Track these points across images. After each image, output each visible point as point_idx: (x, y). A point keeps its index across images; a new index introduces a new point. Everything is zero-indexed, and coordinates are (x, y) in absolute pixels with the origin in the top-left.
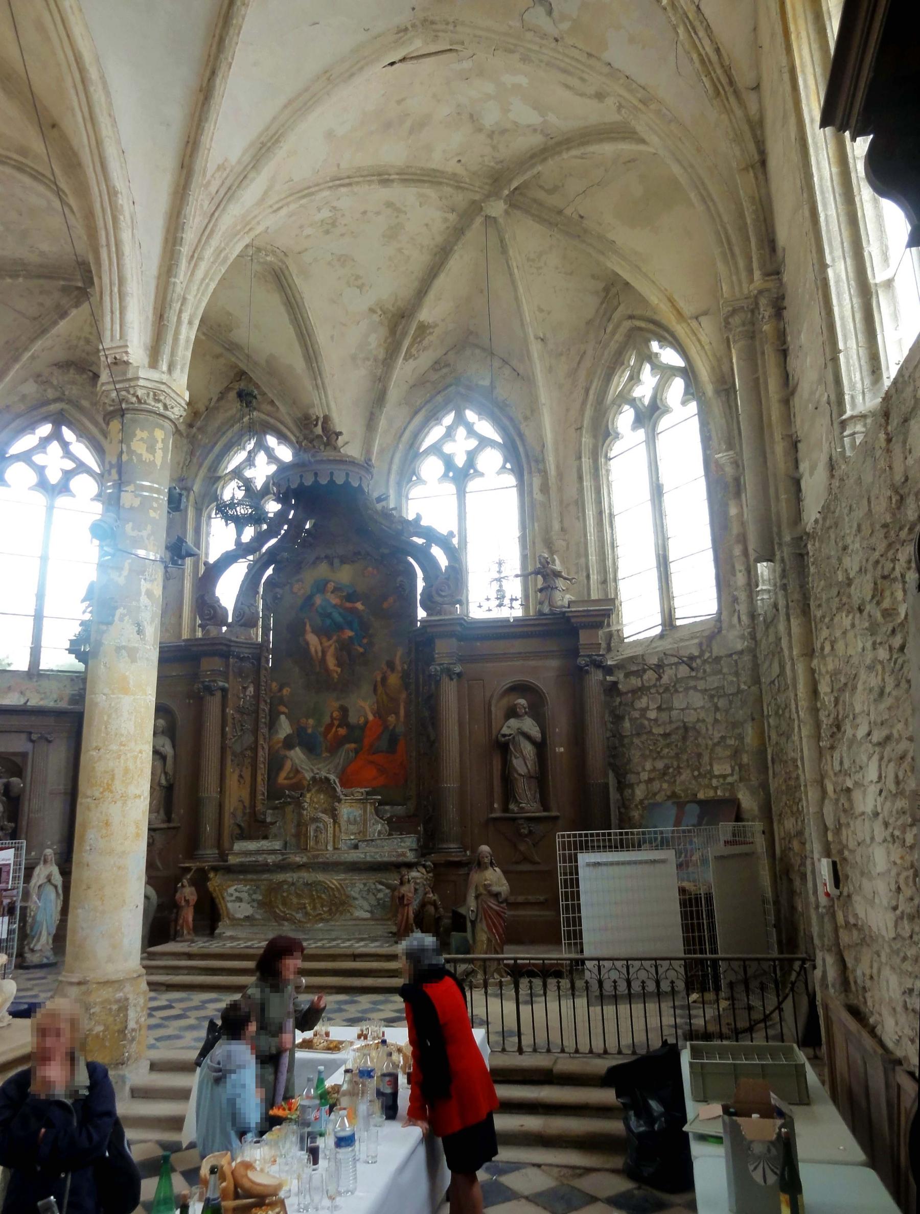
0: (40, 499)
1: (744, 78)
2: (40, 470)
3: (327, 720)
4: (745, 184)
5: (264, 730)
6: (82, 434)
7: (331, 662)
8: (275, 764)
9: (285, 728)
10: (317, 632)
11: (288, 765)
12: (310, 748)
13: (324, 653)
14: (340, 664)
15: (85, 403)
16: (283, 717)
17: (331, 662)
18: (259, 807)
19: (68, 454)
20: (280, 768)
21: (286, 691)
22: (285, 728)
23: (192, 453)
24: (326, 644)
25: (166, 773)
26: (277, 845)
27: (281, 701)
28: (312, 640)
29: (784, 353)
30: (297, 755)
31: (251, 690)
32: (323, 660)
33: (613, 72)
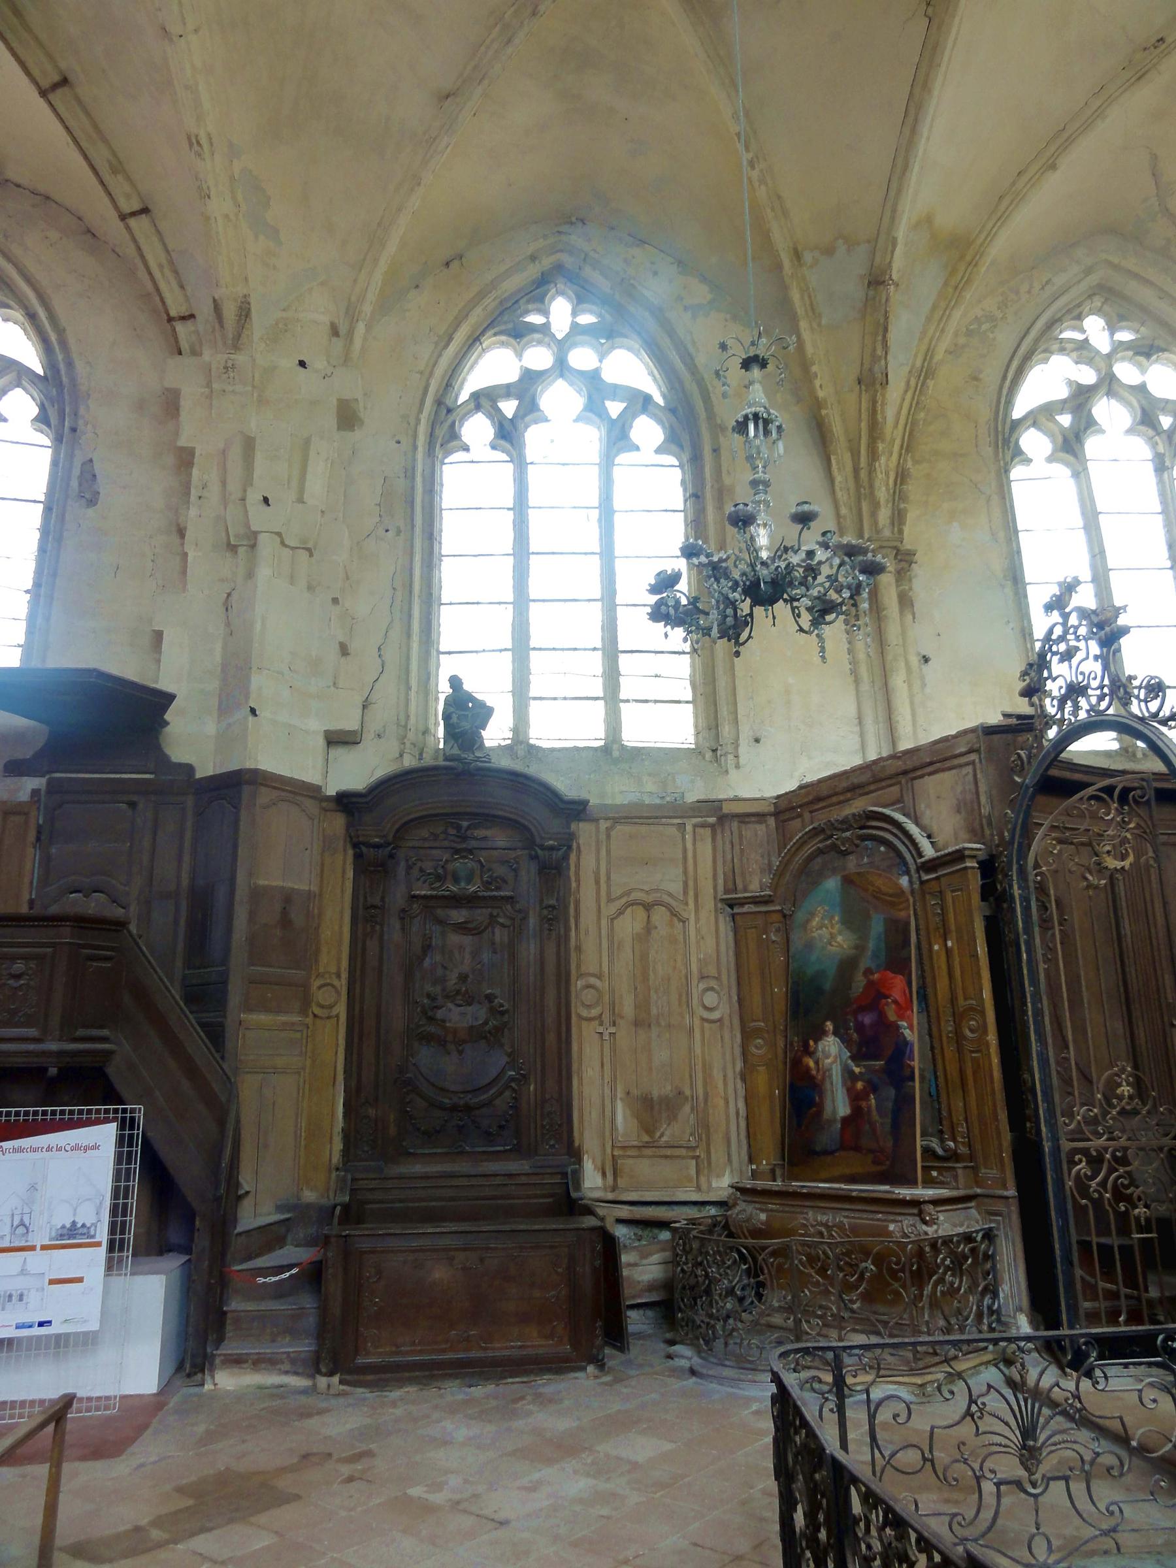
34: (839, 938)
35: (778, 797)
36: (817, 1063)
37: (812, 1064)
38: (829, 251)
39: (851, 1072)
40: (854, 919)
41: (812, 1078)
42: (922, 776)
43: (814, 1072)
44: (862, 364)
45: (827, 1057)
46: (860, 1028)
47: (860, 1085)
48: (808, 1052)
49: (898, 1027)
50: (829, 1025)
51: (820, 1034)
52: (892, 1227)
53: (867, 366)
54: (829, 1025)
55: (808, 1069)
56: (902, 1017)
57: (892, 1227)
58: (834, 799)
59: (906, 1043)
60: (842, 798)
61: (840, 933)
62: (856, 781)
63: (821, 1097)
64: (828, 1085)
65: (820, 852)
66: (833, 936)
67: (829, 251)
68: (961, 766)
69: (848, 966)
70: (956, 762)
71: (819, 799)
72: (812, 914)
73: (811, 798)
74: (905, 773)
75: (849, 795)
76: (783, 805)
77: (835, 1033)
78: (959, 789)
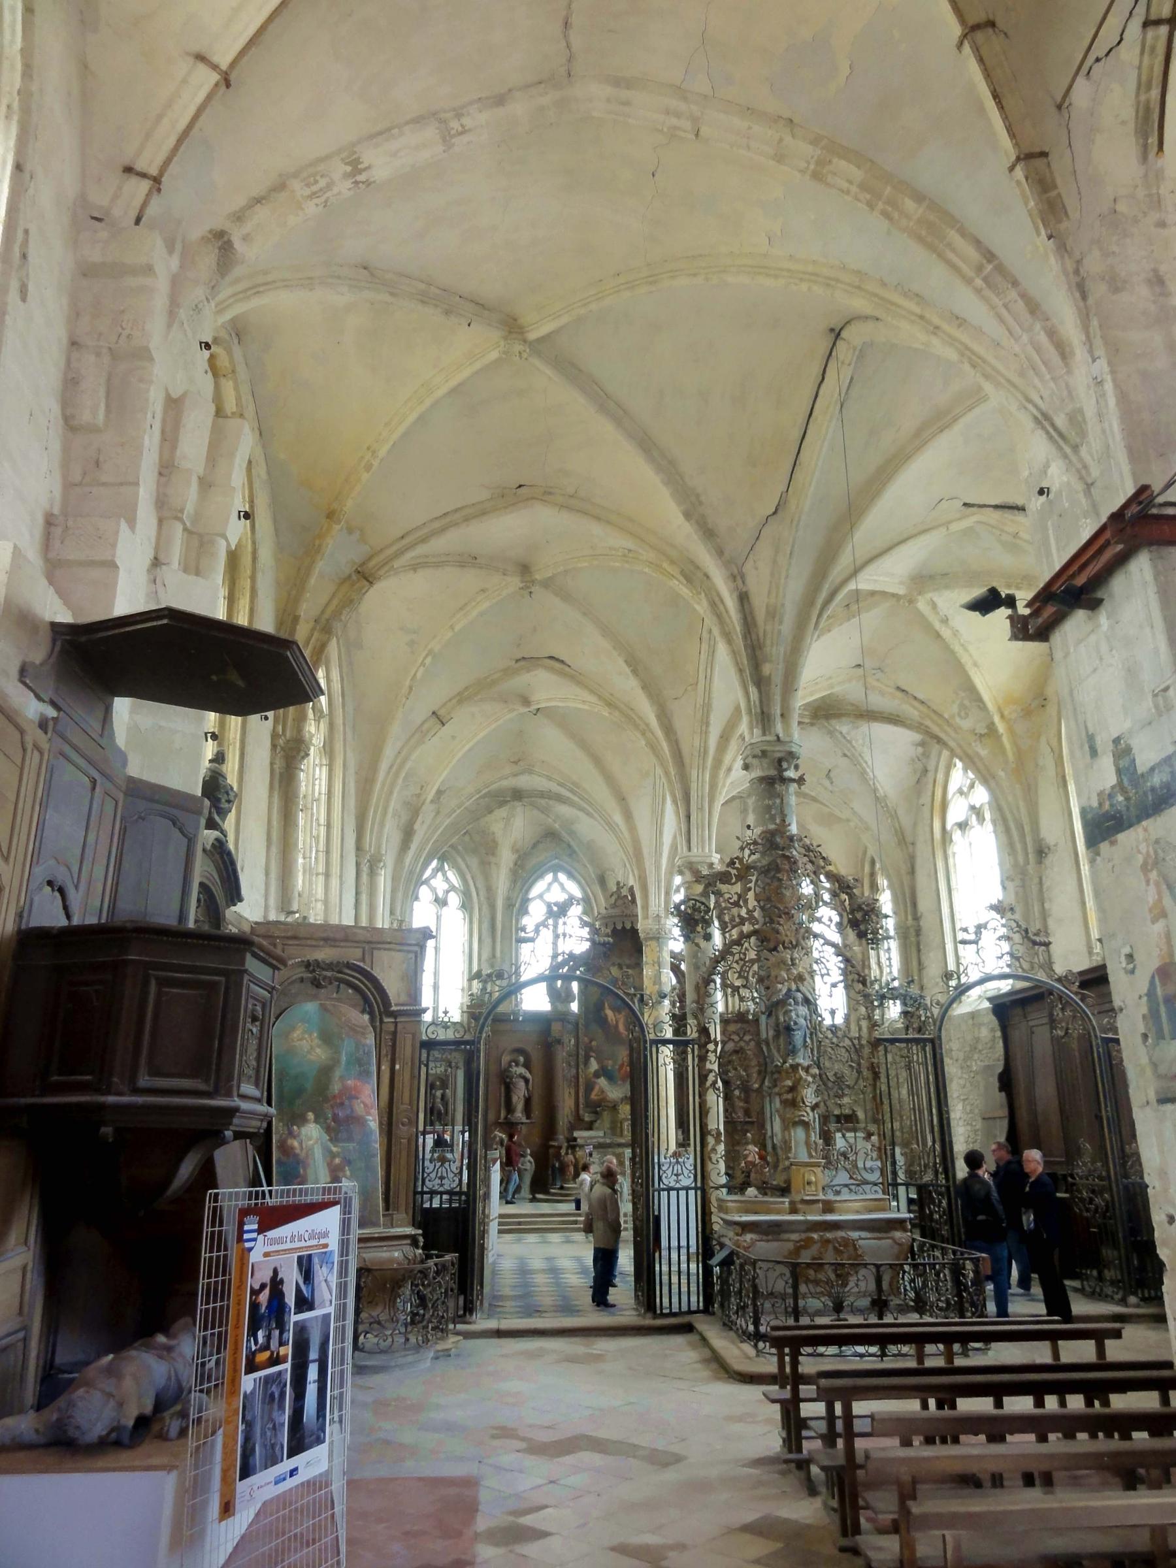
0: (433, 909)
1: (909, 839)
2: (434, 890)
3: (620, 1062)
4: (906, 880)
5: (582, 1066)
6: (455, 866)
7: (621, 1028)
8: (589, 1087)
9: (594, 1065)
10: (613, 1009)
11: (597, 1088)
12: (610, 1078)
13: (617, 1022)
14: (628, 1029)
15: (460, 848)
16: (592, 1059)
17: (621, 1028)
18: (581, 1112)
19: (447, 880)
20: (592, 1089)
21: (594, 1043)
22: (594, 1065)
23: (514, 882)
24: (618, 1016)
25: (527, 1089)
26: (601, 1134)
27: (591, 1049)
28: (609, 1013)
29: (919, 951)
30: (602, 1082)
31: (573, 1041)
32: (617, 1026)
33: (855, 813)
34: (318, 1050)
35: (256, 923)
36: (301, 1144)
37: (296, 1144)
38: (350, 531)
39: (331, 1152)
40: (327, 1038)
41: (296, 1156)
42: (379, 949)
43: (298, 1151)
44: (323, 612)
45: (310, 1139)
46: (335, 1118)
47: (337, 1161)
48: (291, 1134)
49: (366, 1121)
50: (311, 1116)
51: (303, 1120)
52: (396, 1254)
53: (326, 616)
54: (311, 1116)
55: (292, 1148)
56: (369, 1114)
57: (396, 1254)
58: (309, 942)
59: (371, 1132)
60: (314, 943)
61: (319, 1046)
62: (332, 935)
63: (305, 1170)
64: (311, 1162)
65: (302, 980)
66: (312, 1048)
67: (350, 531)
68: (409, 952)
69: (326, 1072)
70: (405, 948)
71: (295, 938)
72: (294, 1028)
73: (289, 934)
74: (370, 942)
75: (321, 943)
76: (261, 931)
77: (316, 1121)
78: (405, 966)
